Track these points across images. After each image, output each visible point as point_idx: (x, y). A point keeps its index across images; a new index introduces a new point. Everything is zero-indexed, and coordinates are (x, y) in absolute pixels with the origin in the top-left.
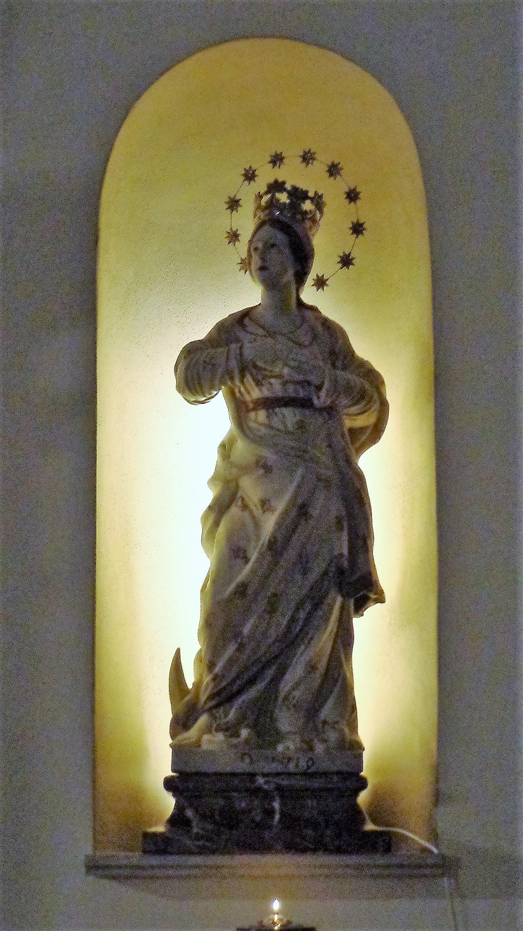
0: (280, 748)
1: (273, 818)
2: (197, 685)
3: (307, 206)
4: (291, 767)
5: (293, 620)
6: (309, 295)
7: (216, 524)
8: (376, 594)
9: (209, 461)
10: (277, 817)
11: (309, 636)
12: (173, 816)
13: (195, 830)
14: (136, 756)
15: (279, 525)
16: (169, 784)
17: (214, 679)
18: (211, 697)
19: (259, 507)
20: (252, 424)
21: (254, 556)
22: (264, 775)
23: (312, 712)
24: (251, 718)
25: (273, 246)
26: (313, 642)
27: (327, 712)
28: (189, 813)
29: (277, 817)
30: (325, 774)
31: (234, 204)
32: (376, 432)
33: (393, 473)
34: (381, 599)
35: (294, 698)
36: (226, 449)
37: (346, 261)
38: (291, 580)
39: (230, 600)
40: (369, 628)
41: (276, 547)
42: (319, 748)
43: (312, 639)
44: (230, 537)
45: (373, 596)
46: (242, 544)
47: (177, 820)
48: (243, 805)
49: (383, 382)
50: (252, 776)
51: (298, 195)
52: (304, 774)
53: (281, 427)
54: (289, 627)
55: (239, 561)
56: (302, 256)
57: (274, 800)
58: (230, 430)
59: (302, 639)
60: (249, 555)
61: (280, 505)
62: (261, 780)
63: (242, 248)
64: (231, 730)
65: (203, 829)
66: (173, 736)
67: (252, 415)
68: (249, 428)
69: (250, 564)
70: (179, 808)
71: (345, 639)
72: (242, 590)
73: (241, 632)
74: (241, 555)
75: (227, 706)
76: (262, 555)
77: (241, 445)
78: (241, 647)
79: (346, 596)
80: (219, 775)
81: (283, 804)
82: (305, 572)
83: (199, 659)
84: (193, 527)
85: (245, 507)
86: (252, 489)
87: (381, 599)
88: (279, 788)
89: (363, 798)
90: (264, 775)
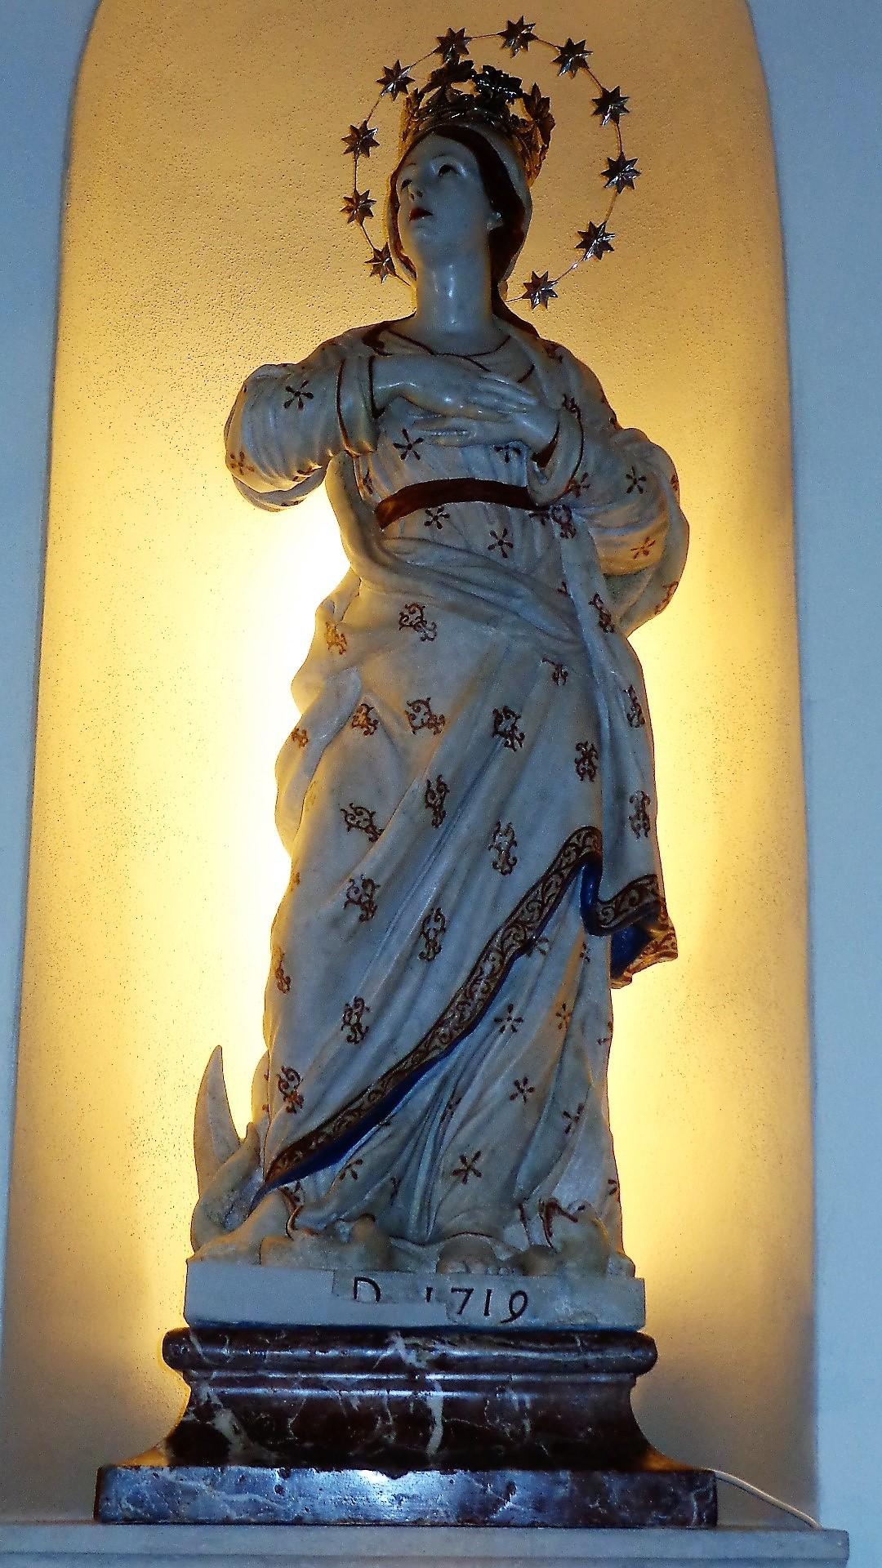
1: (428, 1437)
2: (252, 1129)
3: (517, 109)
4: (474, 1315)
6: (516, 303)
7: (311, 771)
9: (300, 635)
10: (437, 1433)
11: (514, 1016)
12: (182, 1427)
16: (175, 1349)
18: (287, 1153)
20: (390, 544)
22: (406, 1332)
28: (224, 1422)
29: (437, 1433)
31: (361, 141)
32: (661, 584)
33: (698, 665)
35: (478, 1155)
36: (332, 613)
37: (594, 240)
39: (335, 922)
40: (641, 1004)
41: (438, 800)
44: (337, 789)
46: (363, 800)
47: (193, 1443)
50: (378, 1336)
51: (499, 84)
54: (468, 993)
55: (361, 837)
60: (378, 821)
63: (376, 230)
66: (196, 1243)
67: (396, 527)
68: (387, 552)
70: (200, 1409)
71: (591, 1033)
73: (359, 1001)
77: (365, 590)
78: (359, 1034)
79: (593, 925)
82: (507, 865)
83: (264, 1075)
85: (371, 725)
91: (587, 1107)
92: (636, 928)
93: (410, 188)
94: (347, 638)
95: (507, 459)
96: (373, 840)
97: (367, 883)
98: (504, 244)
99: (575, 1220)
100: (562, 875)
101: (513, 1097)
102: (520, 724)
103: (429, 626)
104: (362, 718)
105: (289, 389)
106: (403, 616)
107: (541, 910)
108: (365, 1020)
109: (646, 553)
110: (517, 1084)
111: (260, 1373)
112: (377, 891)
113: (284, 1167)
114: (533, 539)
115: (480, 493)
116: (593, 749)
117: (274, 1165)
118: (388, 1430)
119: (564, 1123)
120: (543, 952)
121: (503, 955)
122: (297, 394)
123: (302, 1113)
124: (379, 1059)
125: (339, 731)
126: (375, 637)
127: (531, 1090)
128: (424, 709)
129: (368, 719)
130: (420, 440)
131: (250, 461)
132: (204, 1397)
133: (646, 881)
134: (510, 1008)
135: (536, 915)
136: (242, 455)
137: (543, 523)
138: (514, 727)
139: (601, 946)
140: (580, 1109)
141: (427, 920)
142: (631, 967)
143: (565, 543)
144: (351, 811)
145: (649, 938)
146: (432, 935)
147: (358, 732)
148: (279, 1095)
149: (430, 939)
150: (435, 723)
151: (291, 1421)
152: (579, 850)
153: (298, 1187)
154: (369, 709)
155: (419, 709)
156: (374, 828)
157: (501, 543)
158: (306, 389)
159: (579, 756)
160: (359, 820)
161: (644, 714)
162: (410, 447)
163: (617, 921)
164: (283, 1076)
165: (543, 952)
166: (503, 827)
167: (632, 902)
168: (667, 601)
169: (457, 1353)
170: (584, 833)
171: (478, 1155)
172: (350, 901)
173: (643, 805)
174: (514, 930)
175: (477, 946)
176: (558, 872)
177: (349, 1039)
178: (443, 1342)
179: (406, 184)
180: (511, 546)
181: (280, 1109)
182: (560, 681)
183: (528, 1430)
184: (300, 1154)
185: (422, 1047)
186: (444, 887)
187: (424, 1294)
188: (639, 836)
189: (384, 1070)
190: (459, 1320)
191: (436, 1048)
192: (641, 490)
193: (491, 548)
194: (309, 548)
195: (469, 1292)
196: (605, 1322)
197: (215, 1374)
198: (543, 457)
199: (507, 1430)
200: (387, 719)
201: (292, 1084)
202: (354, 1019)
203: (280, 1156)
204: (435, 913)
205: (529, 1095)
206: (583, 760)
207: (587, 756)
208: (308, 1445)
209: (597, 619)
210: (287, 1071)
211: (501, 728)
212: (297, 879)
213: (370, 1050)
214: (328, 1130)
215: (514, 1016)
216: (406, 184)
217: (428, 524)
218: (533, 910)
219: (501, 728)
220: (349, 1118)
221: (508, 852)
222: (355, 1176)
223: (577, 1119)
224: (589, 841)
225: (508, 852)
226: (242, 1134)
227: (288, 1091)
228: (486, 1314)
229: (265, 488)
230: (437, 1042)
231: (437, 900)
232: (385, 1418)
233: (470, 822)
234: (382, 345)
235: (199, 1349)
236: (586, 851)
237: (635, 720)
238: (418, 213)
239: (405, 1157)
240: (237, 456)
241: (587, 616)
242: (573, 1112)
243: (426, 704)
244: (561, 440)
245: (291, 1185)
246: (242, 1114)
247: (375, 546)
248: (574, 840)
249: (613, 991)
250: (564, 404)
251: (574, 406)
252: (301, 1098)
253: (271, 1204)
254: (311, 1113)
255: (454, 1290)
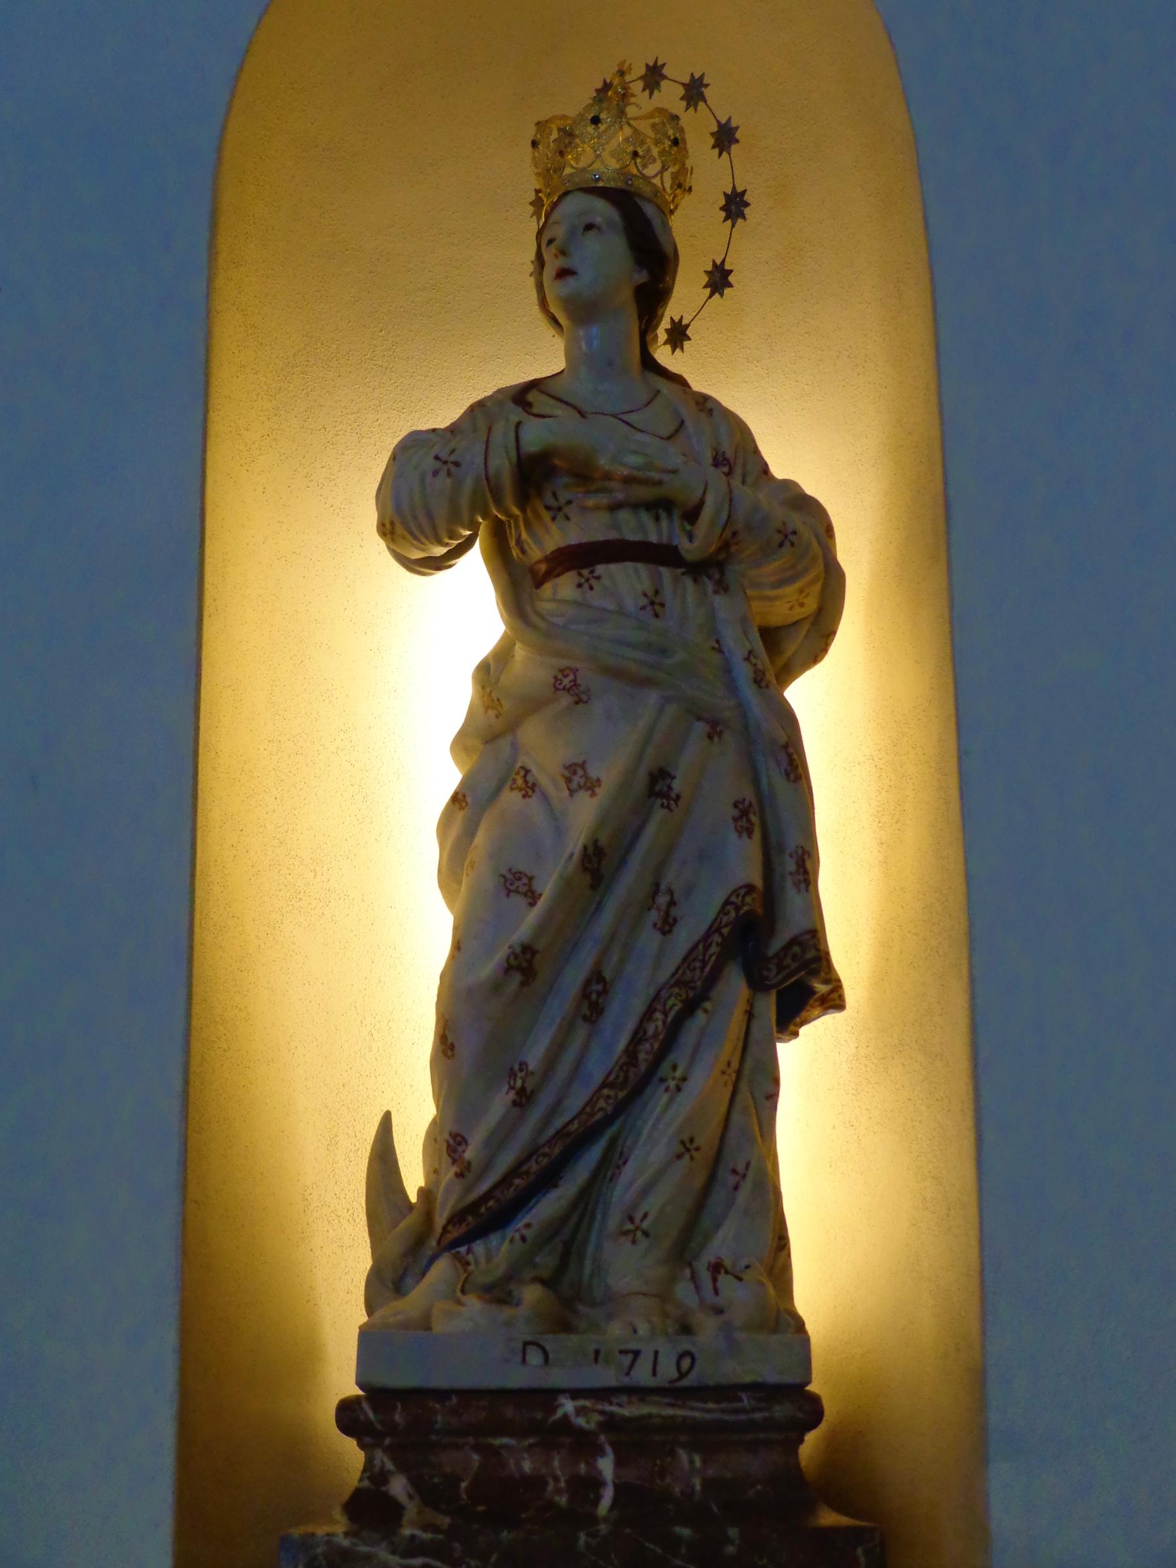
0: (616, 1330)
1: (597, 1501)
2: (421, 1191)
4: (642, 1375)
5: (638, 1037)
6: (663, 355)
7: (470, 832)
8: (827, 981)
9: (454, 701)
10: (608, 1494)
11: (678, 1074)
12: (358, 1493)
13: (407, 1532)
14: (304, 1358)
15: (603, 820)
16: (349, 1416)
17: (460, 1175)
18: (456, 1218)
19: (562, 783)
20: (546, 606)
21: (547, 888)
22: (575, 1394)
23: (683, 1250)
24: (547, 1261)
25: (589, 227)
26: (687, 1087)
27: (721, 1244)
28: (398, 1487)
29: (608, 1494)
30: (727, 1392)
34: (834, 1001)
35: (646, 1215)
36: (488, 674)
38: (636, 934)
39: (495, 987)
40: (809, 1060)
41: (597, 865)
42: (708, 1328)
43: (684, 1079)
45: (821, 988)
46: (521, 866)
47: (369, 1507)
48: (527, 1466)
49: (829, 530)
50: (547, 1397)
52: (675, 1393)
53: (612, 606)
54: (631, 1053)
55: (518, 901)
56: (654, 263)
57: (602, 1453)
58: (505, 637)
59: (662, 1080)
60: (537, 886)
61: (608, 772)
62: (568, 1406)
64: (499, 1293)
65: (426, 1527)
66: (371, 1307)
67: (548, 588)
68: (538, 613)
69: (541, 904)
70: (375, 1475)
72: (524, 964)
73: (523, 1065)
74: (521, 885)
75: (494, 1239)
76: (567, 885)
77: (520, 652)
78: (523, 1099)
79: (757, 985)
80: (468, 1395)
81: (619, 1463)
82: (667, 925)
84: (421, 852)
85: (530, 789)
86: (544, 748)
87: (834, 1001)
88: (611, 1424)
89: (811, 1444)
90: (575, 1394)
91: (753, 1164)
92: (800, 983)
93: (553, 249)
94: (503, 702)
95: (657, 519)
96: (532, 905)
97: (527, 949)
98: (651, 297)
99: (740, 1279)
100: (721, 935)
101: (679, 1157)
102: (676, 785)
103: (582, 688)
104: (520, 781)
105: (437, 458)
106: (555, 678)
107: (702, 971)
108: (529, 1086)
109: (802, 605)
110: (683, 1143)
111: (433, 1438)
112: (538, 956)
113: (455, 1233)
114: (685, 596)
115: (631, 553)
116: (751, 805)
117: (445, 1228)
118: (558, 1491)
119: (732, 1180)
120: (706, 1011)
121: (666, 1014)
122: (445, 462)
123: (470, 1176)
124: (547, 1120)
125: (498, 790)
126: (531, 705)
127: (697, 1149)
128: (580, 772)
129: (526, 782)
130: (569, 502)
131: (399, 529)
132: (377, 1462)
133: (807, 936)
134: (674, 1068)
135: (698, 972)
136: (392, 523)
137: (695, 581)
138: (670, 788)
139: (768, 1006)
140: (748, 1165)
141: (588, 983)
142: (798, 1020)
143: (719, 601)
144: (509, 876)
145: (812, 992)
146: (594, 997)
147: (516, 796)
148: (446, 1158)
149: (593, 1002)
150: (591, 786)
151: (463, 1485)
152: (737, 908)
153: (469, 1251)
154: (527, 771)
155: (575, 773)
156: (533, 892)
157: (652, 603)
158: (453, 458)
159: (736, 813)
160: (515, 884)
161: (800, 769)
162: (560, 509)
163: (780, 977)
164: (451, 1142)
165: (706, 1011)
166: (663, 887)
167: (795, 957)
168: (824, 650)
169: (626, 1412)
170: (742, 892)
171: (646, 1215)
172: (508, 969)
173: (803, 861)
174: (676, 990)
175: (638, 1006)
176: (718, 930)
177: (515, 1104)
178: (611, 1404)
179: (550, 242)
180: (662, 605)
181: (450, 1173)
182: (716, 739)
183: (698, 1488)
184: (470, 1218)
185: (588, 1109)
186: (605, 952)
187: (592, 1356)
188: (799, 891)
189: (551, 1132)
190: (626, 1381)
191: (601, 1109)
192: (792, 544)
193: (643, 608)
194: (459, 612)
195: (636, 1354)
196: (773, 1378)
197: (387, 1441)
198: (692, 515)
199: (677, 1489)
200: (544, 781)
201: (460, 1149)
202: (519, 1083)
203: (450, 1221)
204: (597, 976)
205: (695, 1154)
206: (741, 817)
207: (744, 814)
208: (481, 1508)
209: (751, 675)
210: (454, 1136)
211: (657, 788)
212: (457, 946)
213: (535, 1115)
214: (497, 1194)
215: (678, 1074)
216: (550, 242)
217: (580, 586)
218: (694, 969)
219: (657, 788)
220: (517, 1181)
221: (667, 913)
222: (523, 1239)
223: (744, 1176)
224: (748, 899)
225: (667, 913)
226: (413, 1198)
227: (456, 1156)
228: (654, 1374)
229: (417, 555)
230: (602, 1103)
231: (598, 963)
232: (557, 1479)
233: (628, 883)
234: (530, 405)
235: (371, 1415)
236: (746, 908)
237: (792, 776)
238: (563, 273)
239: (574, 1219)
240: (388, 526)
241: (743, 672)
242: (741, 1168)
243: (583, 765)
244: (710, 500)
245: (463, 1249)
246: (413, 1177)
247: (528, 609)
248: (734, 899)
249: (781, 1048)
250: (715, 459)
251: (725, 459)
252: (469, 1163)
253: (442, 1268)
254: (480, 1177)
255: (621, 1352)
